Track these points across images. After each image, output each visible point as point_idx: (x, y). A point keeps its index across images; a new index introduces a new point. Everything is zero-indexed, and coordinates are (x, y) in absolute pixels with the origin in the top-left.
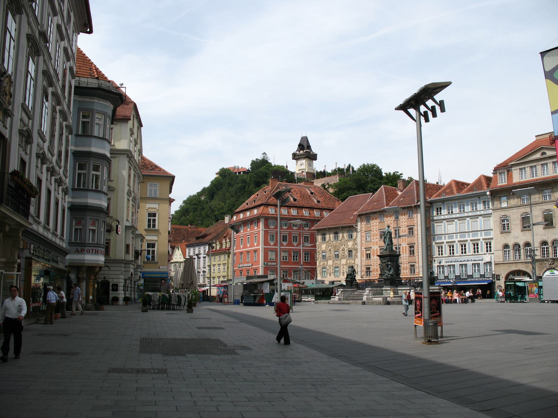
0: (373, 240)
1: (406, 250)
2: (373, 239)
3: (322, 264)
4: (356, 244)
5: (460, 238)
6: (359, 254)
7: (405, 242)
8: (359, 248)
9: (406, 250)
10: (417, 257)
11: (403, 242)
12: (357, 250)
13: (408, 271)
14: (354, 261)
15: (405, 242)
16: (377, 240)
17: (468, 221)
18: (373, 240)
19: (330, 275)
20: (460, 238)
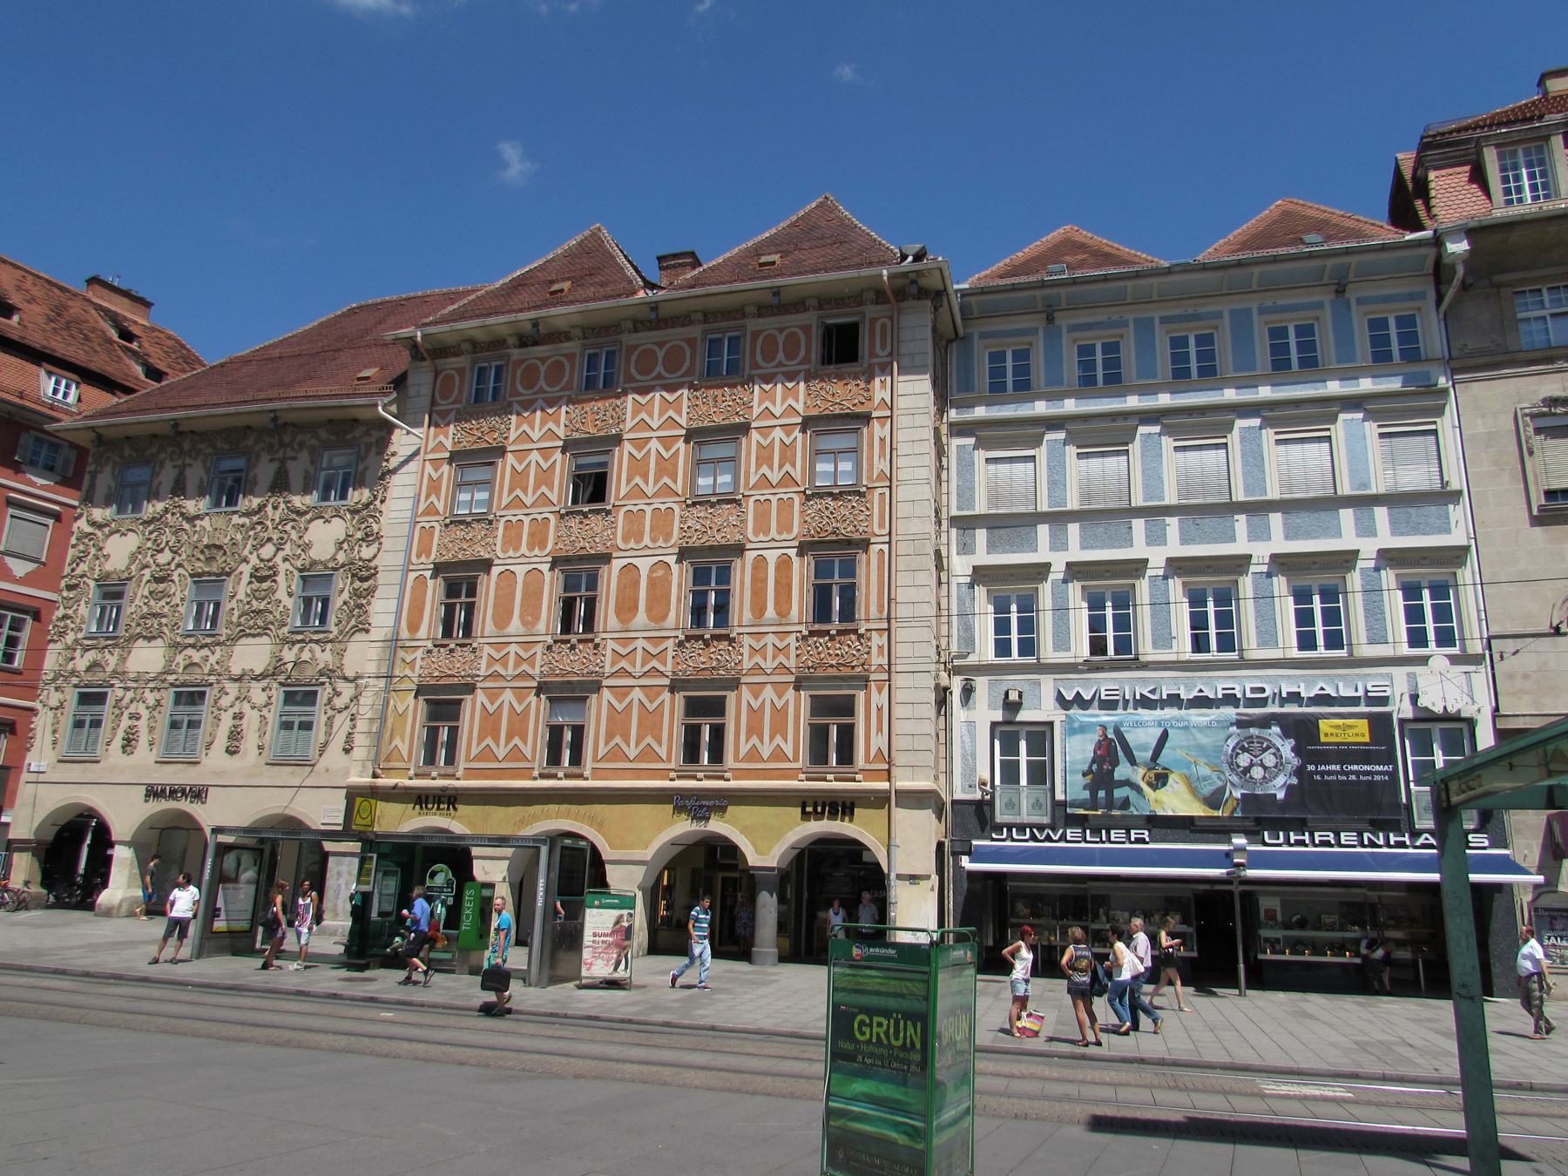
0: (512, 515)
1: (784, 587)
2: (518, 503)
3: (81, 663)
4: (370, 537)
5: (1185, 540)
6: (383, 612)
7: (785, 526)
8: (388, 559)
9: (784, 587)
10: (877, 640)
11: (762, 526)
12: (365, 574)
13: (795, 742)
14: (341, 654)
15: (785, 526)
16: (546, 512)
17: (1250, 438)
18: (512, 515)
19: (129, 743)
20: (1185, 540)
